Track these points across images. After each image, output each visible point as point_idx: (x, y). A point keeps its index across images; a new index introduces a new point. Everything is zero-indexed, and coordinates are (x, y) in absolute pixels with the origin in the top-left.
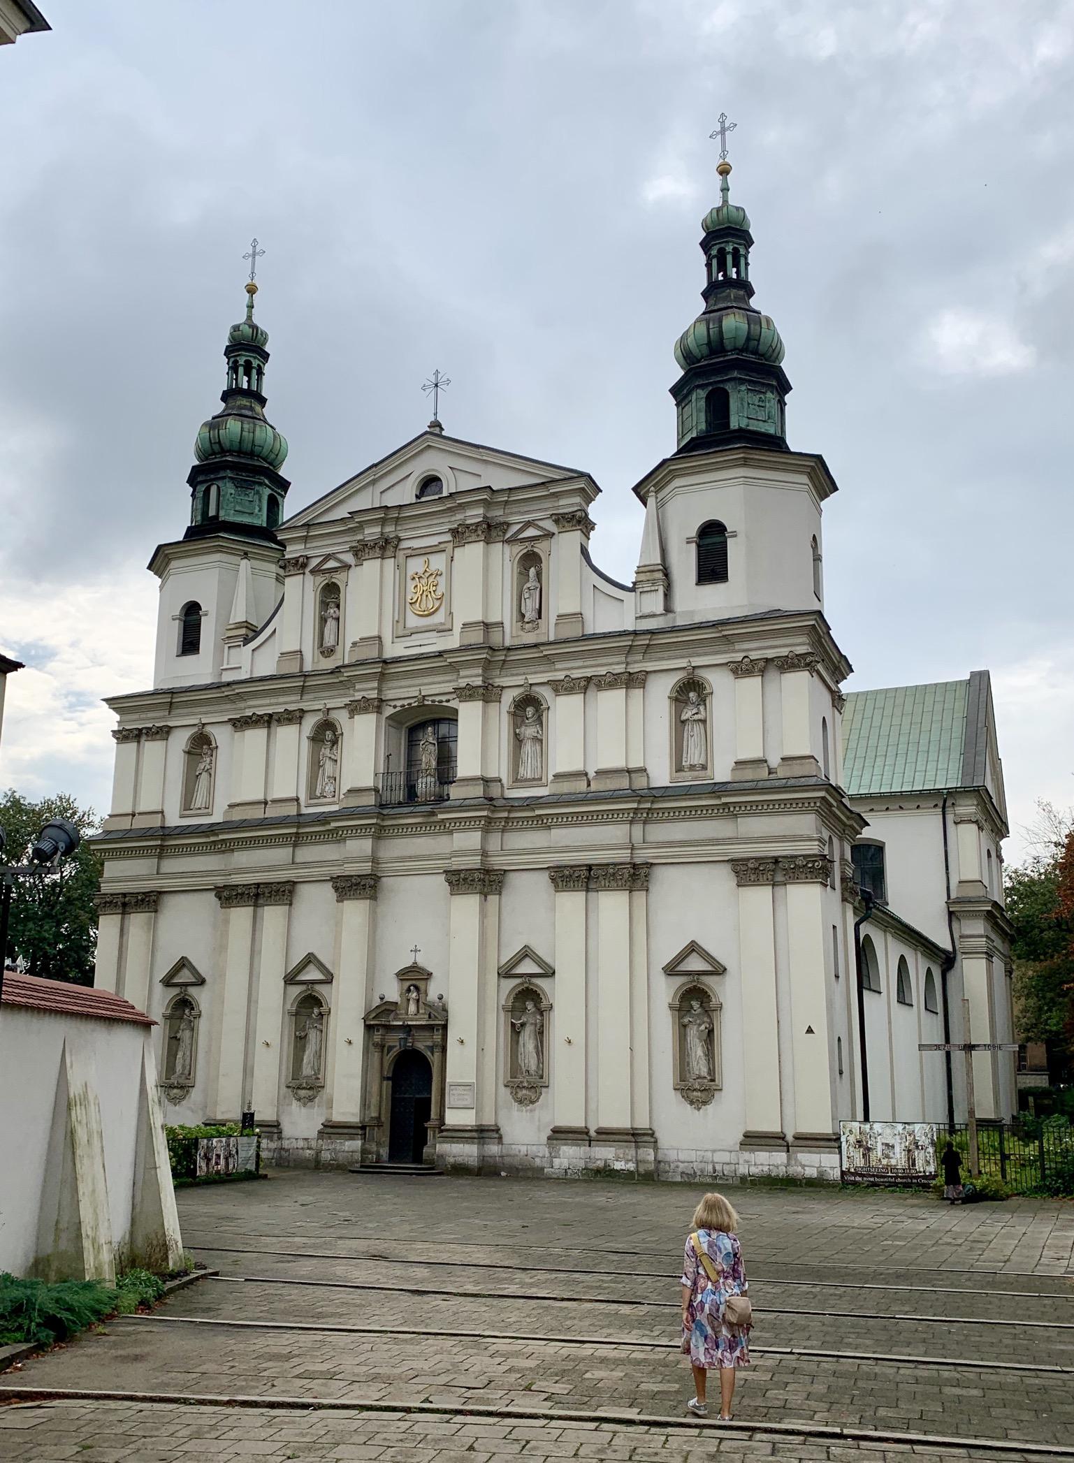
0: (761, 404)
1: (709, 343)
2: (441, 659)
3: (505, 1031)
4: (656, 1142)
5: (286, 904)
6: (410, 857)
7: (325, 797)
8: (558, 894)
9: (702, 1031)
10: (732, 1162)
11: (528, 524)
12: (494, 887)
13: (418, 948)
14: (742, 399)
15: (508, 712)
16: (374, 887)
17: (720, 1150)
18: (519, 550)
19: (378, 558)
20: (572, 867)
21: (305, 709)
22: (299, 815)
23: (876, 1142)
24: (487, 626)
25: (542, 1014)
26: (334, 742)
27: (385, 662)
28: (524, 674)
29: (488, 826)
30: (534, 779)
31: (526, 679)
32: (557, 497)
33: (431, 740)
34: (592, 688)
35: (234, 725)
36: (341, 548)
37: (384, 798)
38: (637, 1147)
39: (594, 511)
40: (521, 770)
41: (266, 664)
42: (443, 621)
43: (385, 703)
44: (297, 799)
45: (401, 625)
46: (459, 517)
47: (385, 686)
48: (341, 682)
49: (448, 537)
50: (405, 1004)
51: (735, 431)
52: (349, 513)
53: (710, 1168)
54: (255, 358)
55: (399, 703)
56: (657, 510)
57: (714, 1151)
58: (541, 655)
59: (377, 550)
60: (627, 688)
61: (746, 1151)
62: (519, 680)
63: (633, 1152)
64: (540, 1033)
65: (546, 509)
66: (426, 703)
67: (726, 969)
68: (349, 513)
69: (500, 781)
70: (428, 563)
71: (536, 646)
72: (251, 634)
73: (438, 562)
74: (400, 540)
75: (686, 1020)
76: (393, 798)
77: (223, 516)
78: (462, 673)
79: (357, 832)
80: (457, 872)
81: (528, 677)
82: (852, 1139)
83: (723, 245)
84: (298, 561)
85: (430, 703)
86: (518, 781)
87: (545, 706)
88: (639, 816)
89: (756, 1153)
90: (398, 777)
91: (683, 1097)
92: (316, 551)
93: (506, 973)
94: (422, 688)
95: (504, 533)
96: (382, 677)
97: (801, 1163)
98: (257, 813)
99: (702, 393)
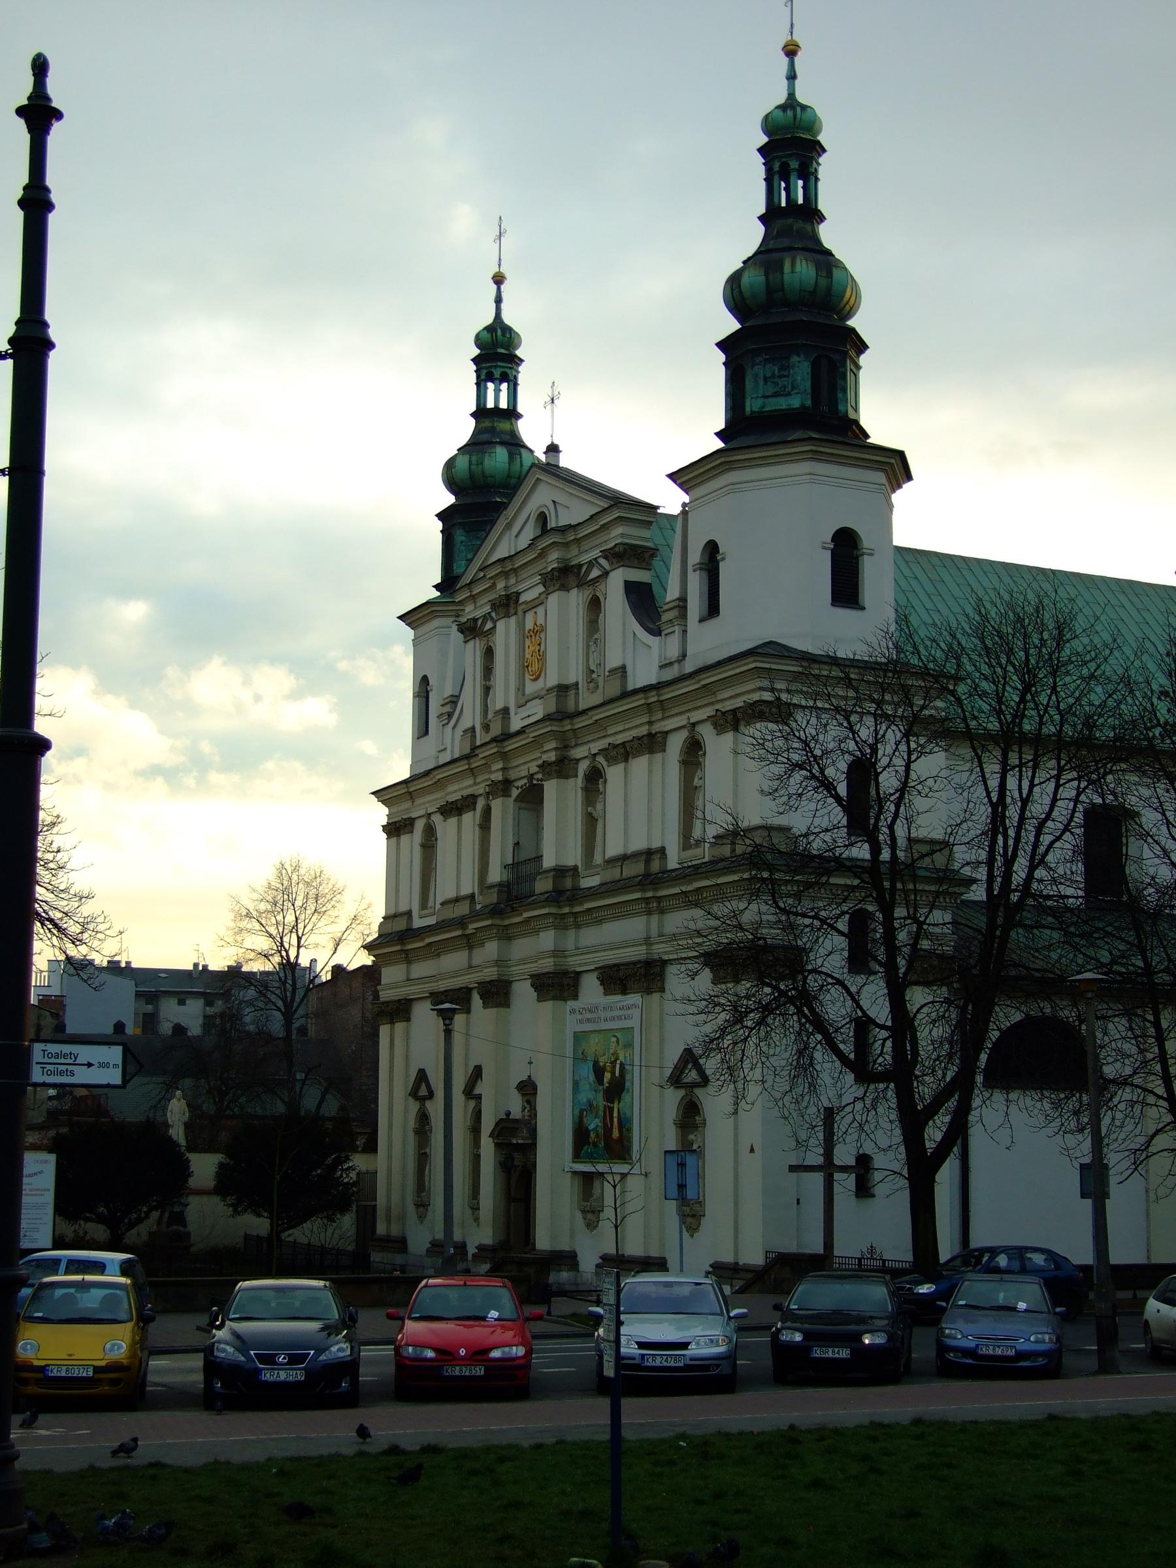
2: (524, 736)
21: (477, 793)
24: (563, 690)
29: (561, 923)
54: (496, 367)
55: (520, 783)
74: (518, 594)
95: (579, 573)
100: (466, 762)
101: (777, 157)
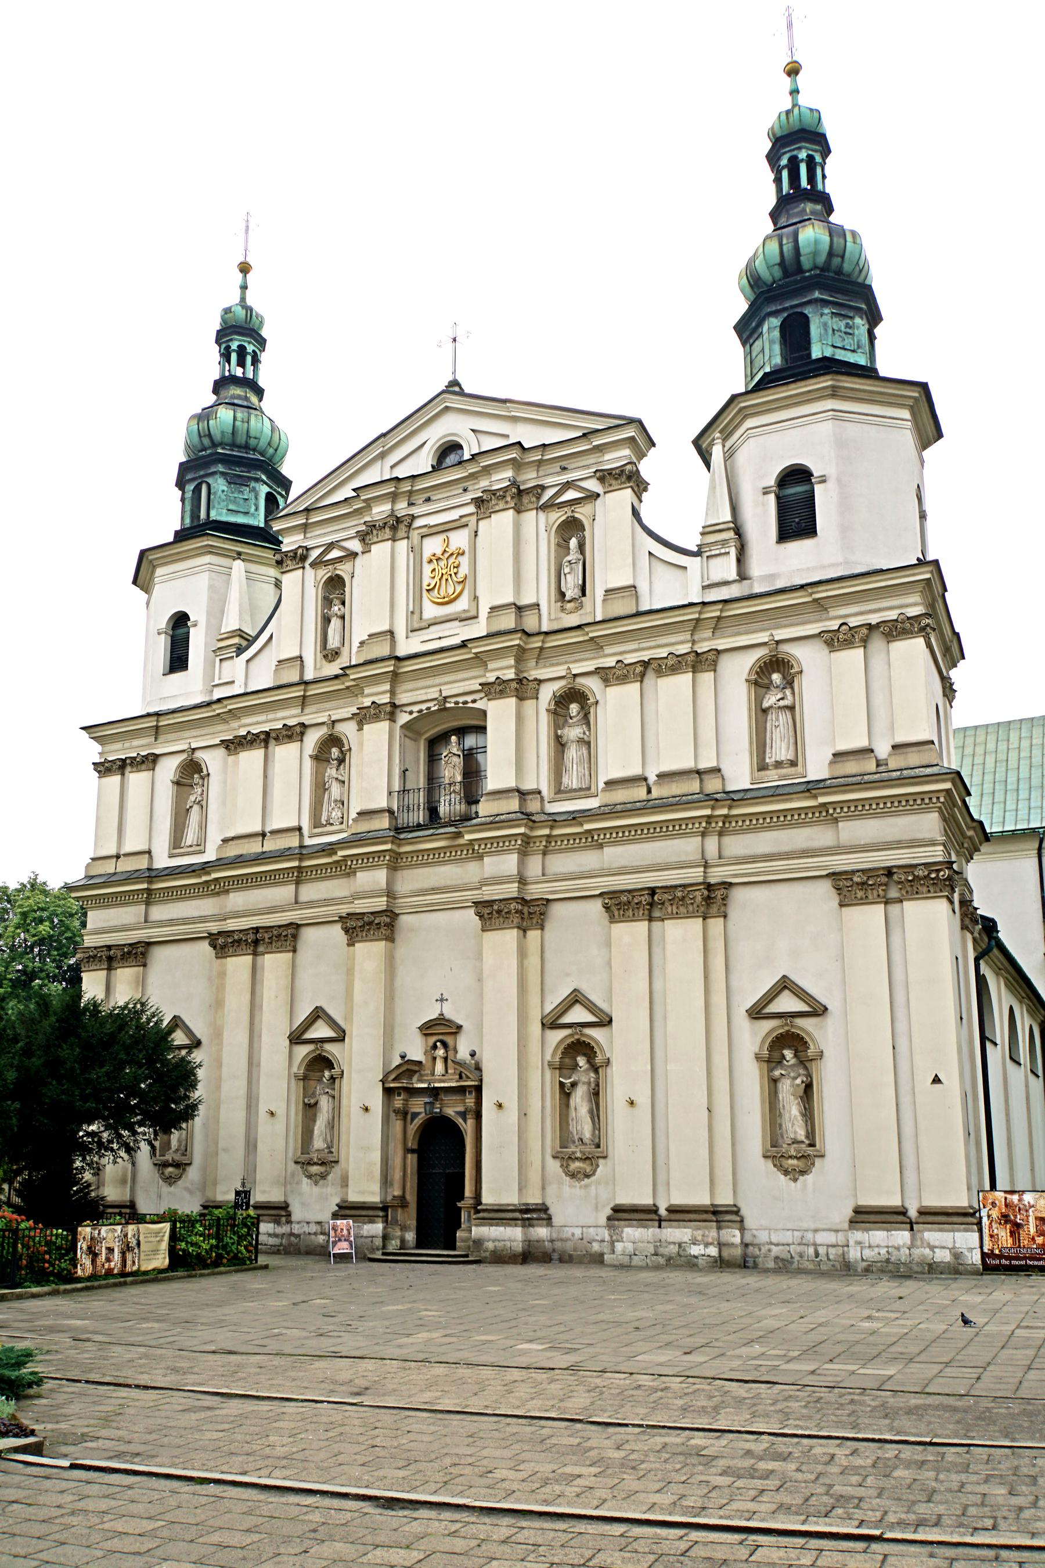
0: (848, 330)
1: (782, 264)
3: (552, 1097)
4: (742, 1221)
5: (289, 951)
6: (433, 889)
7: (332, 824)
8: (613, 925)
9: (798, 1085)
10: (840, 1243)
11: (568, 485)
12: (534, 921)
13: (445, 997)
14: (825, 325)
15: (548, 710)
16: (391, 926)
17: (824, 1230)
18: (557, 517)
19: (388, 540)
20: (630, 891)
21: (307, 723)
22: (302, 847)
23: (1028, 1216)
25: (596, 1070)
26: (341, 761)
27: (398, 659)
28: (566, 663)
29: (526, 847)
30: (581, 789)
31: (569, 668)
32: (601, 451)
33: (455, 750)
34: (650, 676)
35: (227, 748)
36: (347, 534)
37: (400, 821)
38: (719, 1228)
39: (646, 468)
40: (565, 780)
41: (263, 677)
42: (466, 608)
43: (398, 710)
44: (300, 829)
45: (416, 617)
46: (484, 483)
47: (398, 690)
48: (348, 688)
49: (471, 509)
50: (430, 1064)
51: (818, 360)
52: (354, 490)
53: (811, 1251)
56: (725, 461)
57: (816, 1231)
58: (586, 638)
59: (387, 530)
60: (694, 672)
61: (857, 1230)
62: (561, 671)
63: (713, 1234)
64: (595, 1094)
65: (588, 467)
66: (448, 705)
67: (826, 1009)
68: (354, 490)
69: (539, 792)
70: (447, 541)
71: (579, 627)
72: (244, 643)
73: (459, 539)
74: (413, 517)
75: (777, 1073)
76: (411, 820)
77: (214, 515)
78: (491, 666)
79: (369, 861)
80: (490, 903)
81: (571, 666)
82: (995, 1214)
83: (795, 153)
84: (296, 554)
85: (453, 705)
86: (560, 791)
87: (592, 700)
88: (713, 825)
89: (871, 1233)
90: (416, 795)
91: (775, 1166)
92: (317, 540)
93: (551, 1024)
94: (443, 688)
95: (538, 499)
96: (395, 677)
97: (929, 1244)
98: (254, 847)
99: (775, 322)
100: (302, 687)
101: (808, 149)
